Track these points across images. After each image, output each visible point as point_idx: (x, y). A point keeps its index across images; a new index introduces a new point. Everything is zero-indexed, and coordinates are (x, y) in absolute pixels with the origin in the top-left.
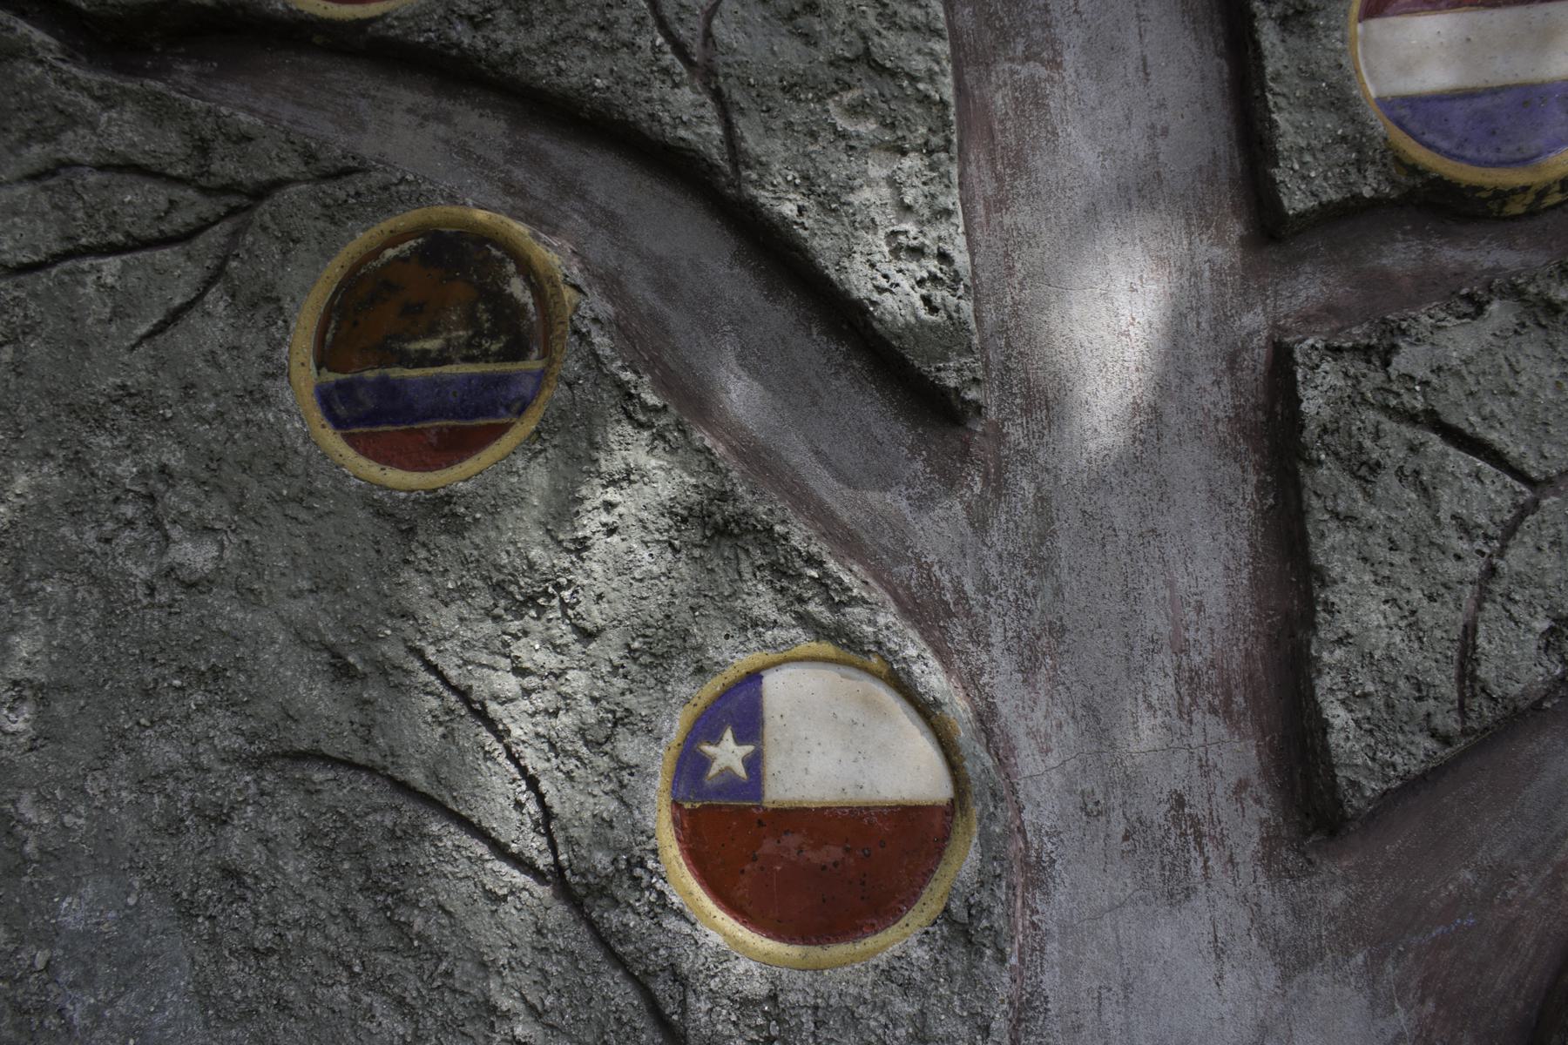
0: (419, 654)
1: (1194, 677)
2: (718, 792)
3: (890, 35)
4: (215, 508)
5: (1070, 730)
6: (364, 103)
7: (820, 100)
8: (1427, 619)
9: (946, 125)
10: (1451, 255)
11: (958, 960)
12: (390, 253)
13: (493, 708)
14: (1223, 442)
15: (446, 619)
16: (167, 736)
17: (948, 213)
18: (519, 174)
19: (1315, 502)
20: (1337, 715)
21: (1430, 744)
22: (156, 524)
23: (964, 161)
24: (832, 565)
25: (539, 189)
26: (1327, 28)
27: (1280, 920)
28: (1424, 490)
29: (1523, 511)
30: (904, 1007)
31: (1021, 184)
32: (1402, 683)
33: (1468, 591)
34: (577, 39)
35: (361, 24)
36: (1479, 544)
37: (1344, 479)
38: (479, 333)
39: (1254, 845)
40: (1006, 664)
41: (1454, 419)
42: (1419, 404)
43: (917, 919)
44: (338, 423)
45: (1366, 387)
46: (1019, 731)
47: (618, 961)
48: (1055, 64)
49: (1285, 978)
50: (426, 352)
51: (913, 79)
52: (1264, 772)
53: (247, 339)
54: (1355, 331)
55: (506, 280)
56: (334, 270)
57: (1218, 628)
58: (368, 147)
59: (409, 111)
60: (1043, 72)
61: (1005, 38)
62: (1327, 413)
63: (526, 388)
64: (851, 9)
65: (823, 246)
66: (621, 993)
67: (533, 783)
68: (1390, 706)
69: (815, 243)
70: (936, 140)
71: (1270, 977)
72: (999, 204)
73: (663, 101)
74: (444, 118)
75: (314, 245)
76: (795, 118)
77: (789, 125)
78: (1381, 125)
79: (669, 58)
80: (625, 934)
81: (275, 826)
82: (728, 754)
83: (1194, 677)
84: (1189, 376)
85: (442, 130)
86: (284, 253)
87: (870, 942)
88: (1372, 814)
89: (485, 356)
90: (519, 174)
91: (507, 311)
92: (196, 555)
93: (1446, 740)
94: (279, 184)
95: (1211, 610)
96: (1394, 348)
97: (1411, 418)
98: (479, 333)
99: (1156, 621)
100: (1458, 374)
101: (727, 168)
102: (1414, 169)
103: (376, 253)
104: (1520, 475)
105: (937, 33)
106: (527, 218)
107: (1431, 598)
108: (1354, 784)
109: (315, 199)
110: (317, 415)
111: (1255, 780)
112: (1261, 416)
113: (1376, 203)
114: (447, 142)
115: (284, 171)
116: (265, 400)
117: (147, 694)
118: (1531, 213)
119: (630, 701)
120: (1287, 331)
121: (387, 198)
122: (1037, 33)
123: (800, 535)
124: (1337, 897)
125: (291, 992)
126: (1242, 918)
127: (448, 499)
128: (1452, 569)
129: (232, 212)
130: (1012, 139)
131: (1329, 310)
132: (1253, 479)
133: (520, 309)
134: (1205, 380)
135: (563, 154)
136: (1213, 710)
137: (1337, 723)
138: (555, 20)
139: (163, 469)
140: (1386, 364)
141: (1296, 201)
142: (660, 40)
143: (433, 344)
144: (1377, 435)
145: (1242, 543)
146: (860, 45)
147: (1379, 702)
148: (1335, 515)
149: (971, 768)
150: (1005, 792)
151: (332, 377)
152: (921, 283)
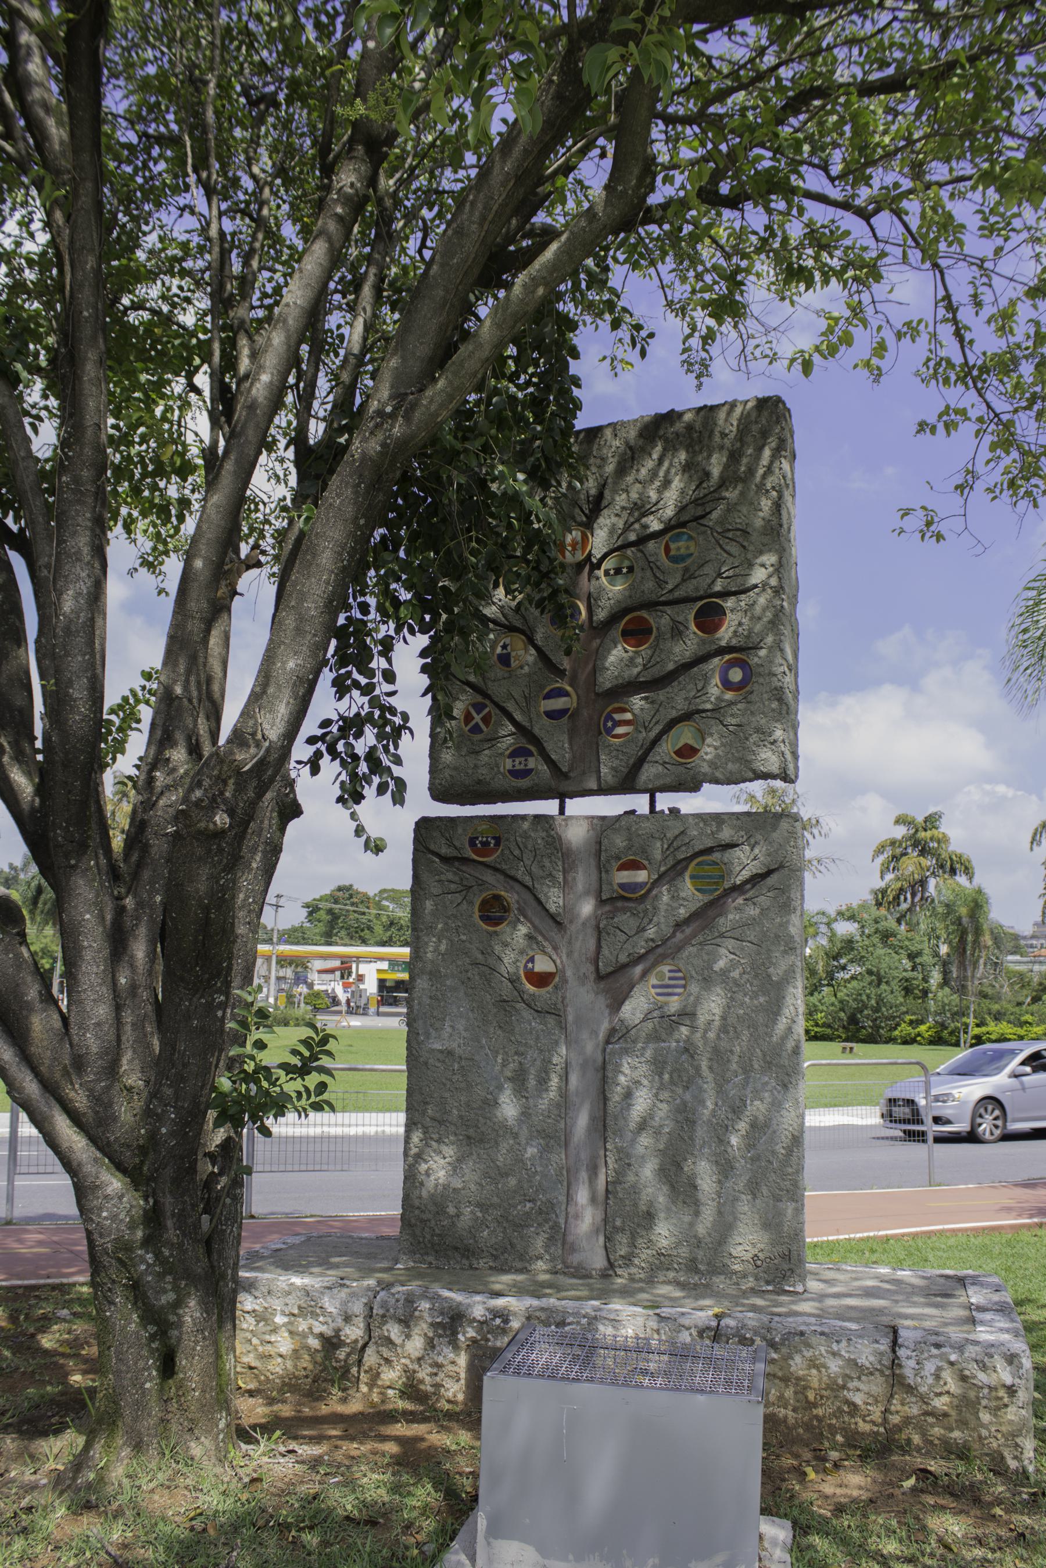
78: (616, 887)
91: (504, 907)
92: (464, 938)
121: (488, 889)
123: (540, 938)
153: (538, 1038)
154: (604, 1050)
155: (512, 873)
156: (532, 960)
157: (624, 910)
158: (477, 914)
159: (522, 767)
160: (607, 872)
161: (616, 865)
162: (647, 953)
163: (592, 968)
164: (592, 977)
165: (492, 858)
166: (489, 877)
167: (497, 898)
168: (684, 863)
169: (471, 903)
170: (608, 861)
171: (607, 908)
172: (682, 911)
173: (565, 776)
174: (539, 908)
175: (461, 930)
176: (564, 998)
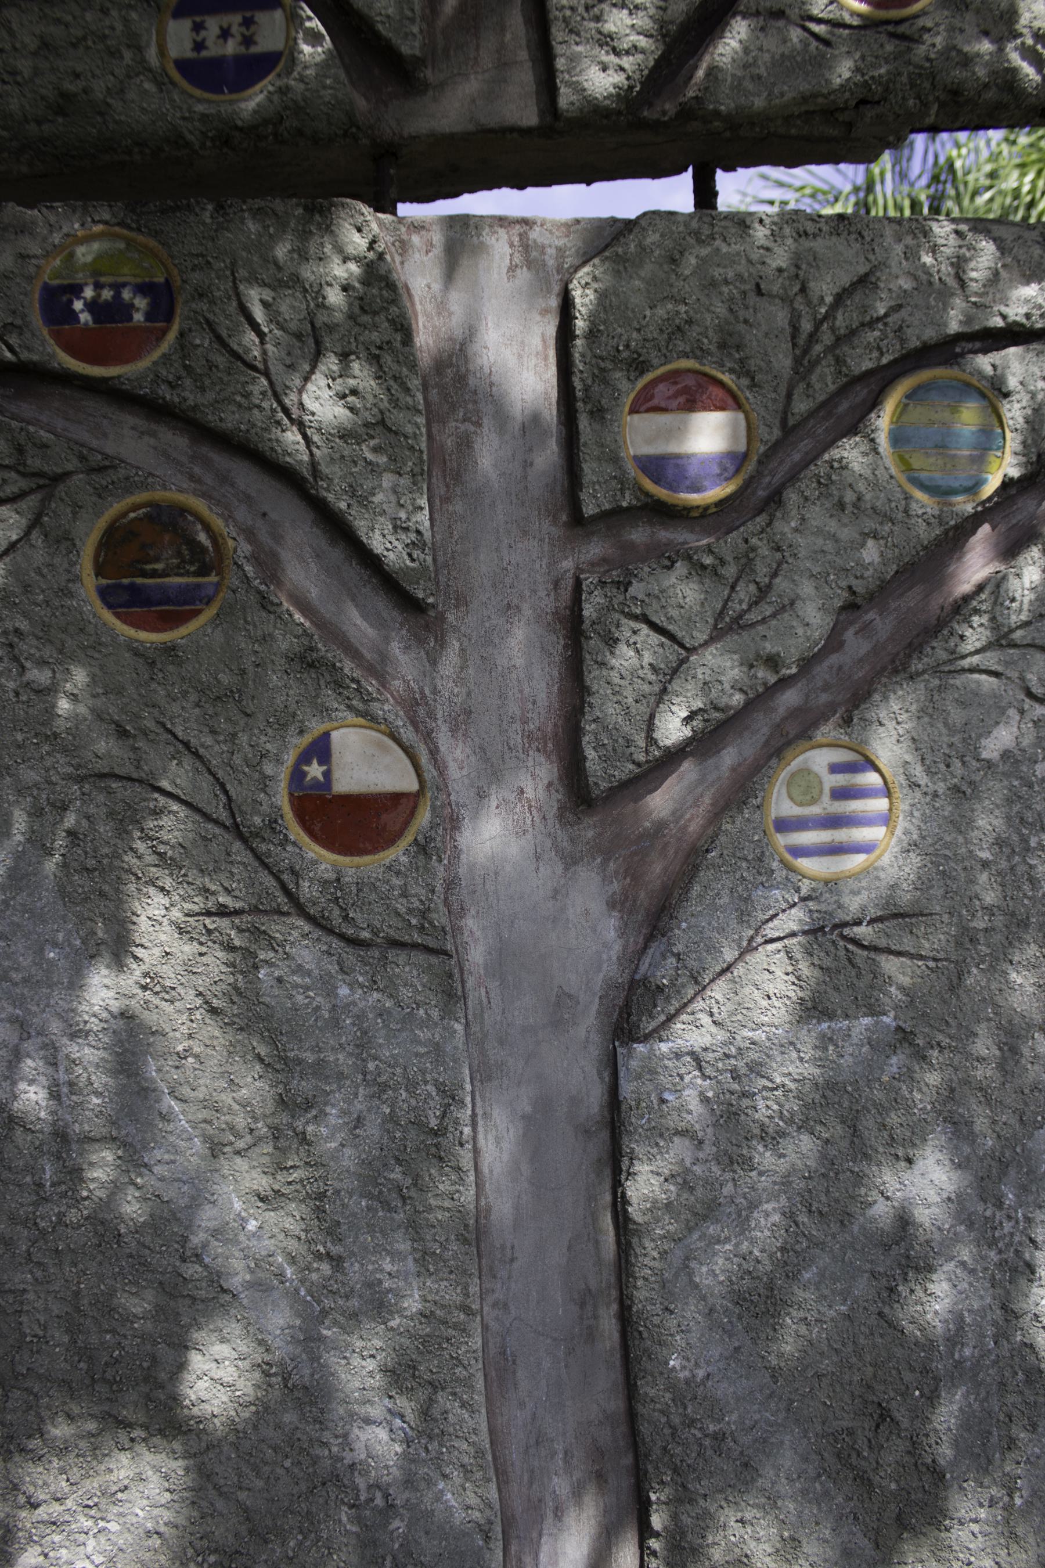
0: (163, 725)
1: (530, 735)
2: (312, 787)
3: (395, 411)
4: (48, 652)
5: (473, 758)
6: (105, 422)
7: (358, 444)
8: (633, 711)
9: (422, 461)
10: (664, 535)
11: (421, 860)
12: (132, 515)
13: (201, 751)
14: (549, 624)
15: (176, 708)
16: (32, 768)
17: (421, 508)
18: (197, 470)
19: (588, 656)
20: (590, 753)
21: (631, 766)
22: (15, 659)
23: (430, 476)
24: (364, 683)
25: (209, 479)
26: (611, 420)
27: (565, 844)
28: (637, 651)
29: (682, 662)
30: (396, 882)
31: (458, 490)
32: (620, 740)
33: (653, 699)
34: (230, 400)
35: (105, 380)
36: (661, 677)
37: (601, 645)
38: (183, 561)
39: (555, 810)
40: (444, 728)
41: (654, 619)
42: (638, 611)
43: (404, 843)
44: (110, 606)
45: (615, 602)
46: (449, 759)
47: (266, 866)
48: (479, 424)
49: (566, 869)
50: (155, 571)
51: (406, 437)
52: (560, 778)
53: (57, 561)
54: (614, 573)
55: (197, 533)
56: (102, 523)
57: (543, 712)
58: (110, 448)
59: (133, 428)
60: (472, 428)
61: (453, 407)
62: (594, 615)
63: (210, 591)
64: (375, 396)
65: (361, 525)
66: (270, 882)
67: (223, 786)
68: (614, 750)
69: (356, 523)
70: (417, 470)
71: (560, 869)
72: (447, 500)
73: (278, 441)
74: (153, 434)
75: (90, 510)
76: (346, 453)
77: (343, 457)
78: (632, 471)
79: (280, 415)
80: (269, 854)
81: (92, 810)
82: (315, 770)
83: (530, 735)
84: (535, 591)
85: (152, 441)
86: (74, 513)
87: (381, 855)
88: (607, 797)
89: (188, 574)
90: (197, 470)
93: (639, 765)
94: (67, 474)
95: (540, 704)
96: (630, 583)
97: (635, 618)
98: (183, 561)
99: (514, 709)
100: (658, 597)
101: (311, 479)
102: (647, 494)
103: (125, 514)
104: (682, 645)
105: (419, 411)
106: (205, 495)
107: (637, 701)
108: (596, 784)
109: (90, 484)
110: (98, 603)
111: (556, 782)
112: (568, 612)
113: (628, 509)
114: (155, 448)
115: (70, 467)
116: (71, 595)
117: (19, 747)
118: (703, 516)
119: (268, 746)
120: (583, 571)
121: (129, 486)
122: (470, 406)
123: (348, 667)
124: (590, 834)
125: (106, 888)
126: (548, 843)
127: (174, 648)
128: (647, 688)
129: (40, 487)
130: (455, 464)
131: (604, 560)
132: (562, 642)
133: (204, 550)
134: (542, 593)
135: (221, 460)
136: (539, 750)
137: (590, 757)
138: (217, 388)
139: (17, 631)
140: (626, 590)
141: (589, 509)
142: (275, 405)
143: (159, 566)
144: (618, 626)
145: (556, 673)
146: (379, 416)
147: (610, 748)
148: (596, 662)
149: (427, 776)
150: (442, 787)
151: (104, 582)
152: (407, 545)
153: (363, 1044)
154: (612, 1065)
158: (89, 583)
159: (231, 48)
160: (598, 413)
161: (629, 391)
162: (749, 706)
165: (143, 364)
168: (861, 393)
170: (601, 376)
171: (595, 549)
172: (871, 552)
174: (337, 554)
175: (26, 647)
176: (451, 884)
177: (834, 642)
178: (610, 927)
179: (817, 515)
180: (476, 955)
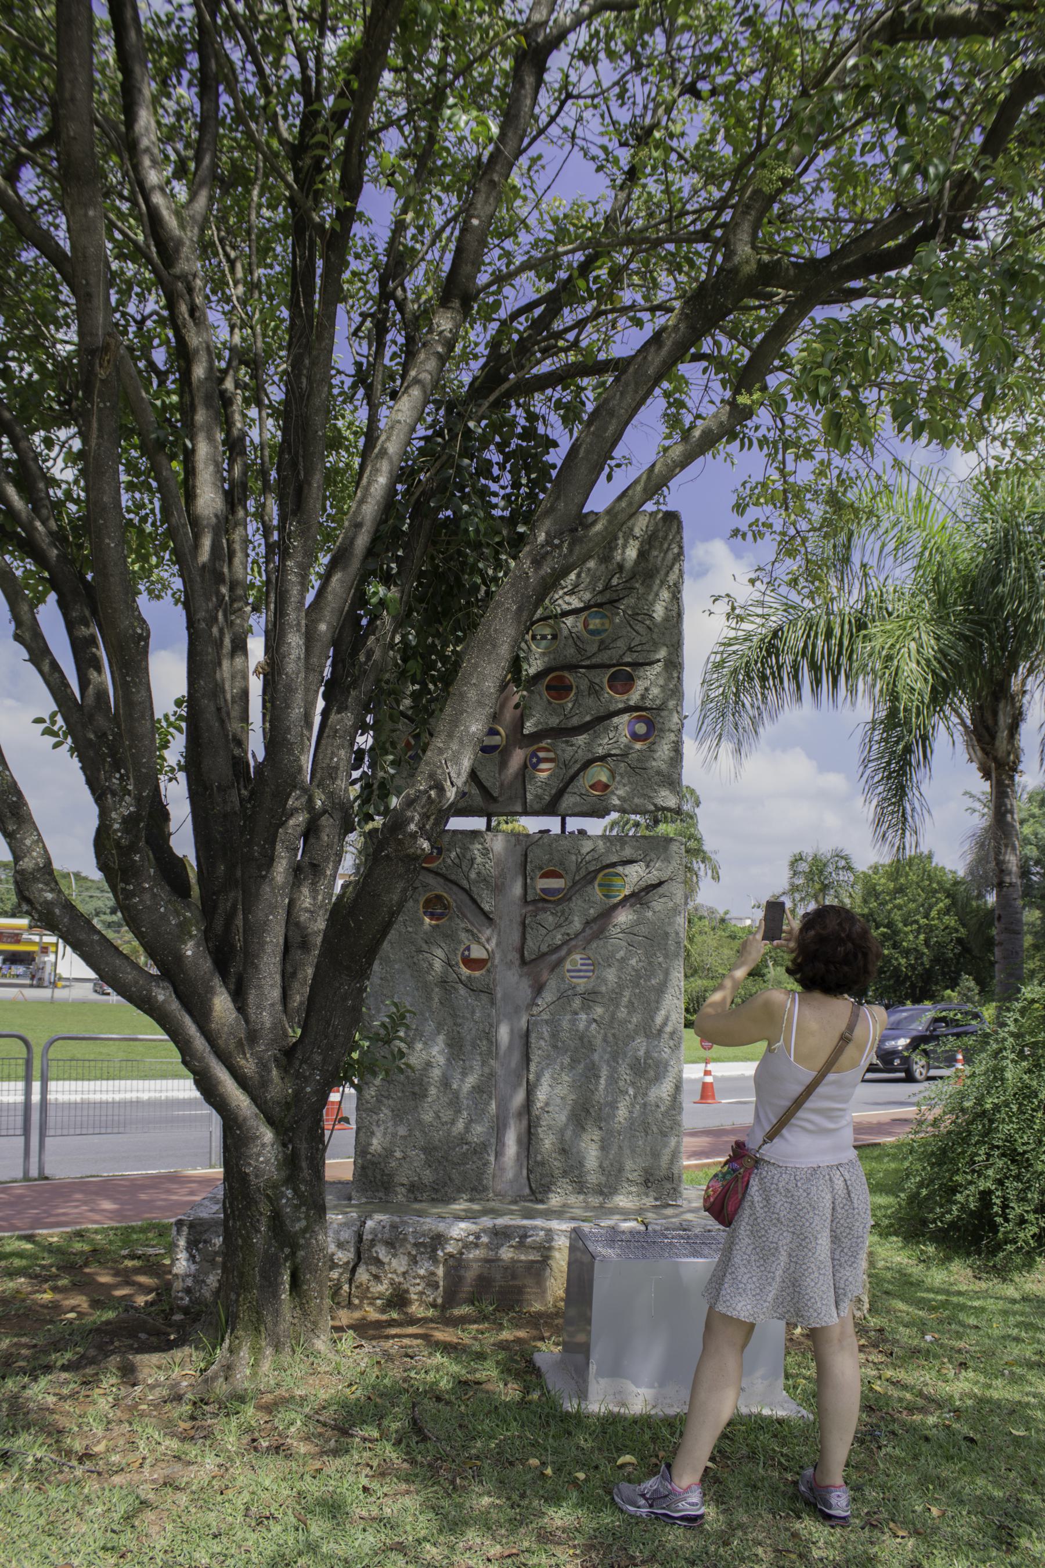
155: (453, 877)
156: (468, 948)
157: (545, 910)
158: (421, 910)
162: (563, 944)
163: (517, 956)
164: (517, 963)
166: (431, 880)
167: (439, 897)
169: (417, 901)
171: (531, 908)
172: (592, 911)
173: (495, 800)
174: (473, 907)
177: (583, 930)
178: (529, 991)
179: (579, 902)
180: (499, 996)
